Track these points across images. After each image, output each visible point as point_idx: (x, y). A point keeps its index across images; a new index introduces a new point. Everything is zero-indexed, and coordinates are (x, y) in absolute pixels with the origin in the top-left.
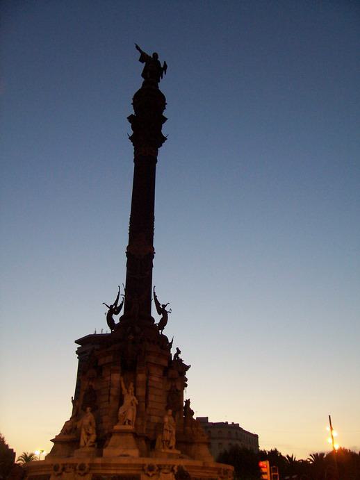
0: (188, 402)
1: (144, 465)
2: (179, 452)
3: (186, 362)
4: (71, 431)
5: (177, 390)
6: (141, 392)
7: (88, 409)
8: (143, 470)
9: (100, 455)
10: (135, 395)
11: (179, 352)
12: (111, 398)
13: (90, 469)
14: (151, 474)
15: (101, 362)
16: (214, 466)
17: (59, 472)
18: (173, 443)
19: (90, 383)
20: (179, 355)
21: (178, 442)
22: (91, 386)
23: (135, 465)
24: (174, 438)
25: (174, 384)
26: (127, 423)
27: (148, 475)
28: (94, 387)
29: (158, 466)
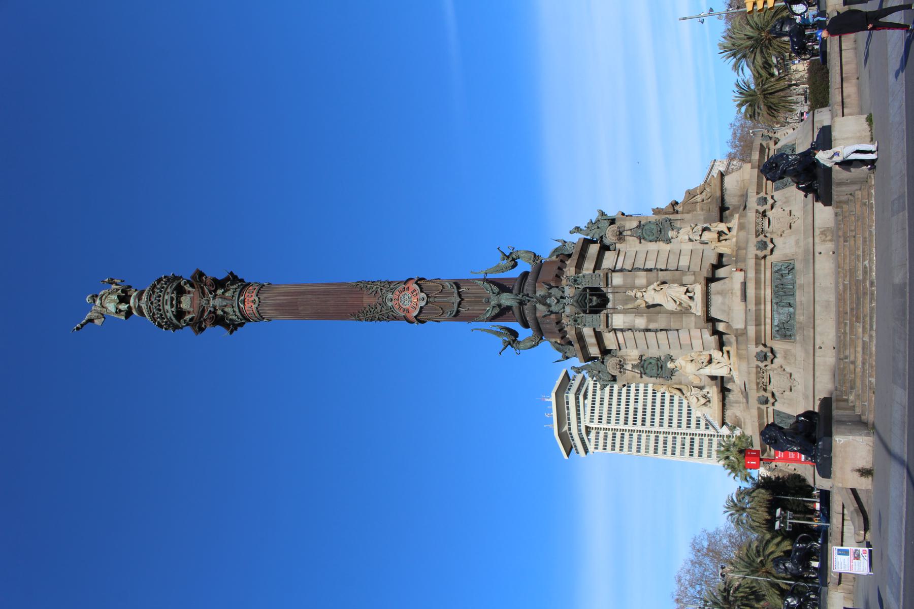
0: (657, 211)
1: (757, 257)
2: (737, 216)
3: (594, 217)
4: (705, 397)
5: (639, 226)
6: (641, 279)
7: (670, 365)
8: (765, 257)
9: (741, 334)
10: (647, 287)
11: (578, 229)
12: (652, 326)
13: (765, 345)
14: (771, 246)
15: (594, 351)
16: (758, 153)
17: (769, 395)
18: (722, 227)
19: (629, 367)
20: (583, 227)
21: (721, 221)
22: (634, 366)
23: (757, 271)
24: (714, 225)
25: (629, 233)
26: (691, 295)
27: (772, 251)
28: (635, 363)
29: (757, 236)
